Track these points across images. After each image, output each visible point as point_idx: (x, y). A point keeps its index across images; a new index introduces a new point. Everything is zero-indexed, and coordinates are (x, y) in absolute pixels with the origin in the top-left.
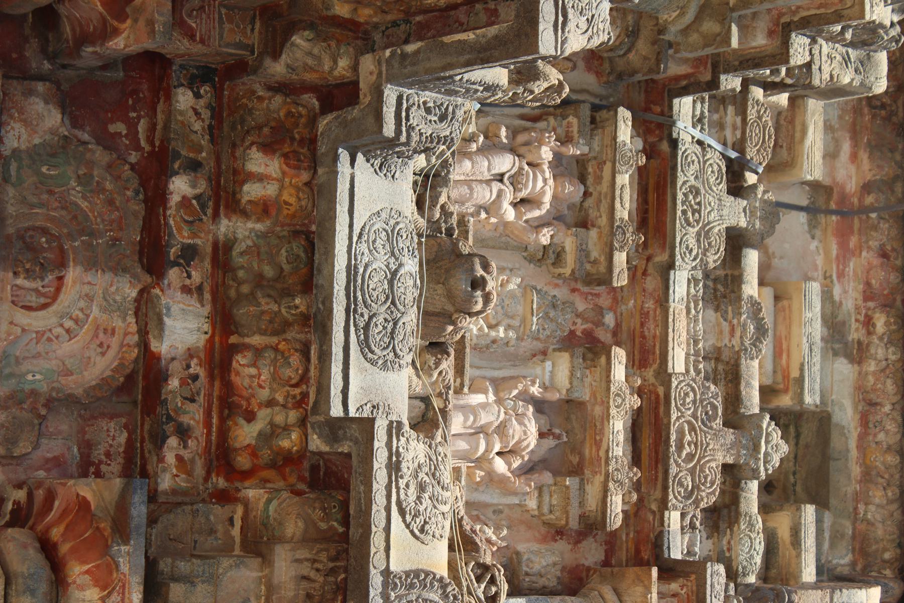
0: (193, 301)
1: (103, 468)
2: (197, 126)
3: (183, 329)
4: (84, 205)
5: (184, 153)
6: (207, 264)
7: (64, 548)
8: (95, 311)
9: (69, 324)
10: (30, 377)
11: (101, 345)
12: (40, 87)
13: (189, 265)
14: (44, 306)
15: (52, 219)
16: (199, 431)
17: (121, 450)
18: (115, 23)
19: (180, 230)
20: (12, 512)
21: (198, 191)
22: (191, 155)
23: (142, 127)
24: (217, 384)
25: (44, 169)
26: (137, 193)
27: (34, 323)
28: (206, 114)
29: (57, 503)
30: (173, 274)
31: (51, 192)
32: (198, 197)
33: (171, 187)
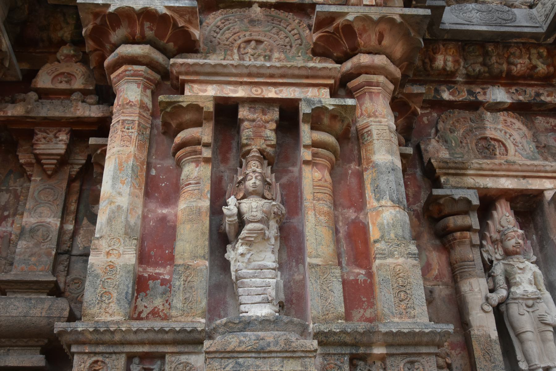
0: (488, 91)
1: (553, 124)
3: (499, 95)
5: (433, 95)
6: (473, 86)
8: (500, 126)
10: (532, 149)
11: (512, 124)
12: (422, 147)
13: (475, 93)
16: (535, 89)
19: (463, 96)
21: (446, 89)
22: (433, 92)
24: (520, 82)
25: (454, 145)
26: (450, 112)
30: (481, 98)
32: (449, 90)
33: (447, 99)
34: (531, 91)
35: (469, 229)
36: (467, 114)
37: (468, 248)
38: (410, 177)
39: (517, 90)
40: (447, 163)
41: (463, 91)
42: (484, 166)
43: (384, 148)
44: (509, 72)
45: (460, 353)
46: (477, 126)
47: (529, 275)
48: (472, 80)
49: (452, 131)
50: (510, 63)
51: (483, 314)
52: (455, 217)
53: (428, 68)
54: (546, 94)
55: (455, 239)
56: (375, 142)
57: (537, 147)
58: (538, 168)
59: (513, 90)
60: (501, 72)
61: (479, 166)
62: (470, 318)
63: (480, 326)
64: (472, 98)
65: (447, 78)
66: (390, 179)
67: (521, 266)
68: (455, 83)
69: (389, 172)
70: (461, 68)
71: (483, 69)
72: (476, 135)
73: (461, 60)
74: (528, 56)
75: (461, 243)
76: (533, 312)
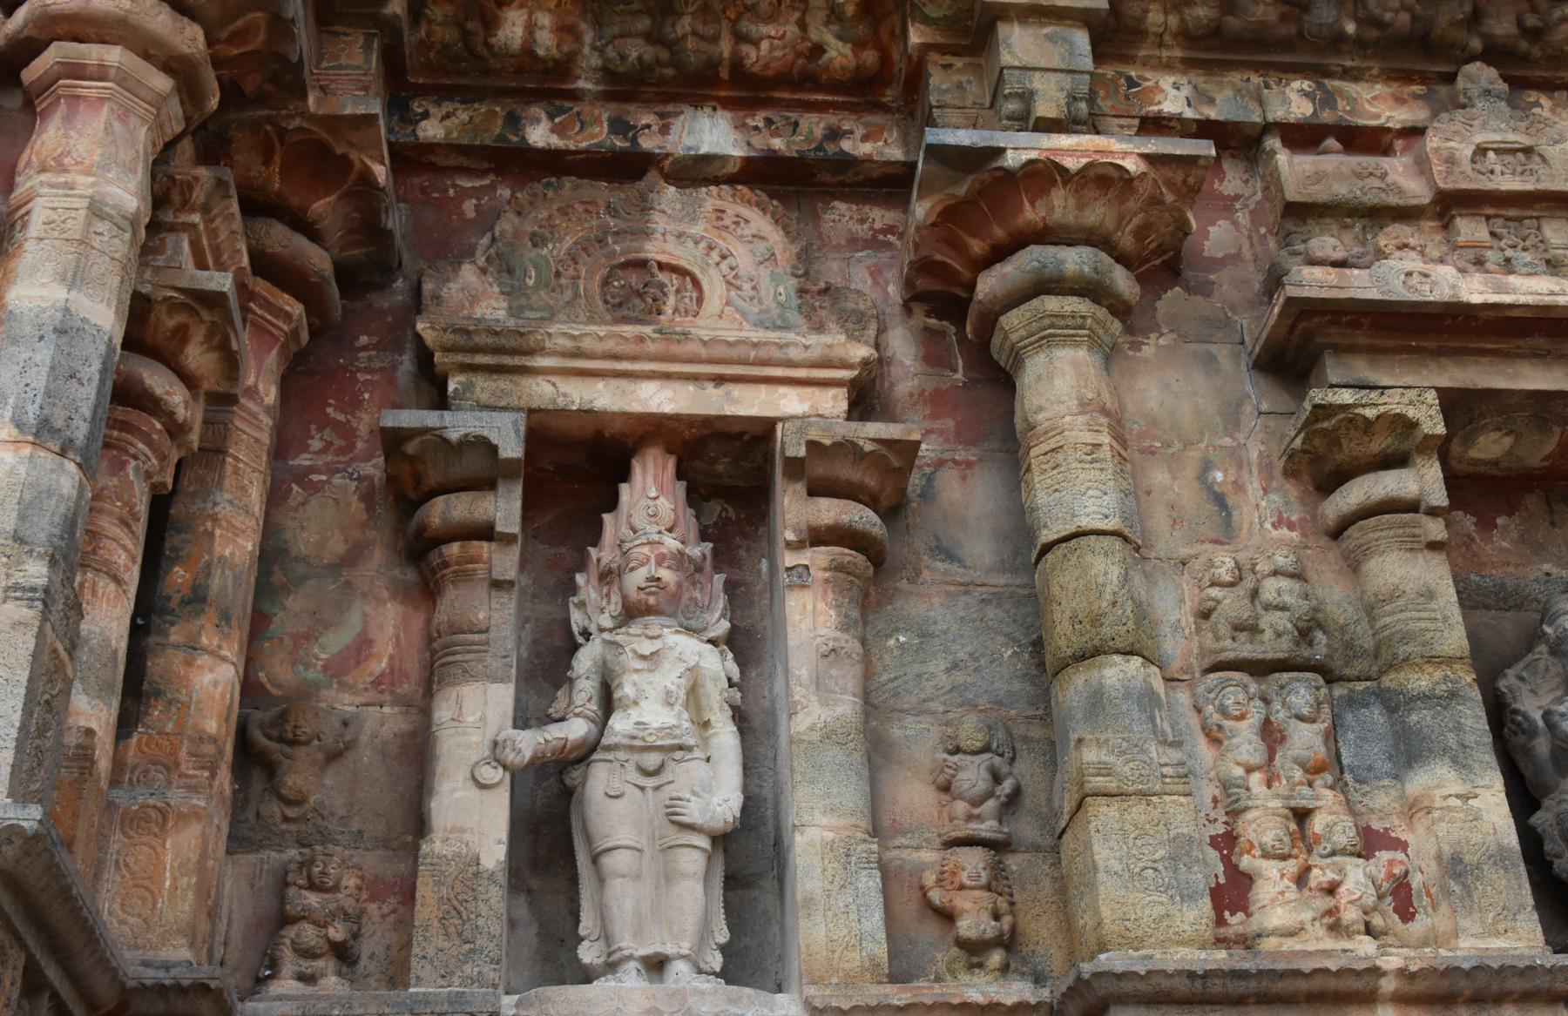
0: (677, 124)
1: (878, 225)
2: (464, 116)
3: (712, 133)
4: (569, 242)
5: (498, 131)
6: (632, 107)
7: (999, 233)
8: (697, 230)
9: (715, 256)
10: (783, 298)
11: (737, 223)
12: (428, 286)
13: (634, 127)
14: (696, 283)
15: (591, 274)
16: (831, 118)
17: (854, 207)
18: (353, 176)
19: (593, 136)
20: (939, 318)
21: (543, 116)
22: (500, 122)
23: (467, 184)
24: (777, 95)
25: (531, 282)
26: (548, 185)
27: (718, 292)
28: (447, 107)
29: (938, 257)
30: (648, 143)
31: (558, 274)
32: (551, 117)
33: (541, 144)
34: (814, 125)
35: (486, 532)
36: (601, 191)
37: (482, 591)
38: (376, 377)
39: (769, 122)
40: (467, 332)
41: (598, 121)
42: (587, 344)
43: (50, 266)
44: (737, 63)
45: (394, 911)
46: (623, 225)
47: (670, 678)
48: (625, 87)
49: (537, 241)
50: (740, 38)
51: (475, 793)
52: (453, 496)
53: (480, 48)
54: (860, 132)
55: (446, 565)
56: (30, 246)
57: (801, 292)
58: (763, 353)
59: (758, 120)
60: (713, 64)
61: (569, 344)
62: (433, 805)
63: (454, 829)
64: (619, 143)
65: (546, 82)
66: (38, 358)
67: (647, 647)
68: (575, 96)
69: (41, 338)
70: (586, 50)
71: (650, 53)
72: (612, 254)
73: (584, 26)
74: (797, 15)
75: (464, 576)
76: (657, 788)
